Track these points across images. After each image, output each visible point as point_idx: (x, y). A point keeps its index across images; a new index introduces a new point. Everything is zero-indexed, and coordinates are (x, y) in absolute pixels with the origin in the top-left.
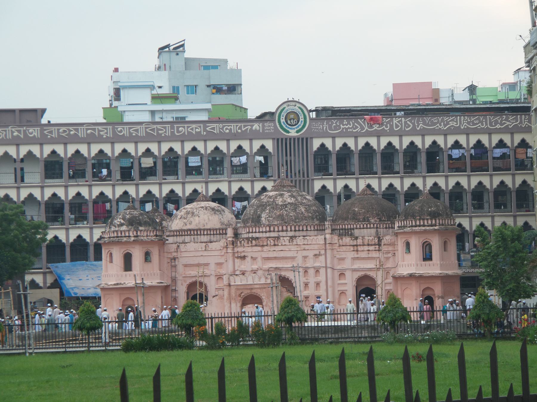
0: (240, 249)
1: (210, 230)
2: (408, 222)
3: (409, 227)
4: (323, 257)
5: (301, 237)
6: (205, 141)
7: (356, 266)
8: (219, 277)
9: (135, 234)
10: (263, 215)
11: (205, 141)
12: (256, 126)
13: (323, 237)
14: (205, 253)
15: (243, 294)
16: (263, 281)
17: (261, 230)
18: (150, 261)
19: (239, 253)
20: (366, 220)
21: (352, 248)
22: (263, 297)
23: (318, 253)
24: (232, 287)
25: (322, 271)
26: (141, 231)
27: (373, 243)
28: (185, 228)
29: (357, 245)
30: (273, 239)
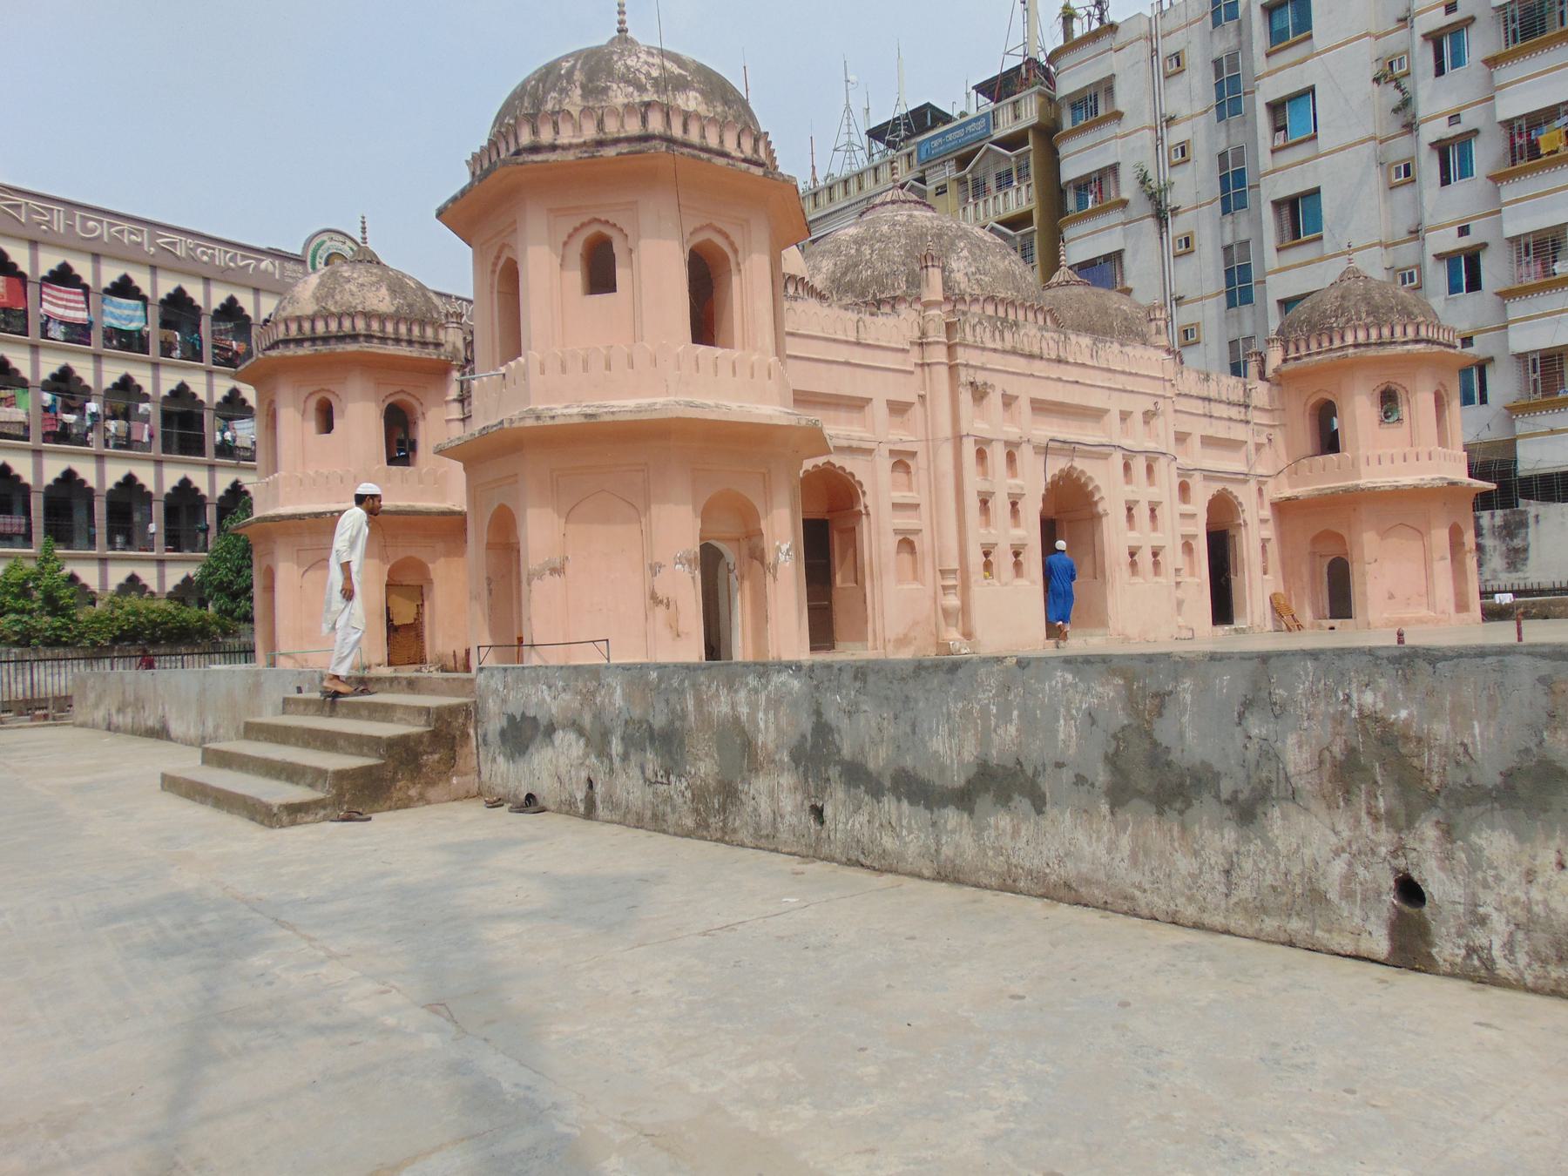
0: (974, 357)
2: (1398, 330)
3: (1405, 343)
5: (1116, 346)
7: (1209, 464)
8: (902, 462)
9: (747, 144)
10: (954, 265)
12: (266, 264)
14: (857, 355)
19: (971, 371)
21: (1199, 407)
23: (1152, 408)
25: (1161, 466)
27: (1234, 398)
29: (1210, 400)
30: (1056, 336)
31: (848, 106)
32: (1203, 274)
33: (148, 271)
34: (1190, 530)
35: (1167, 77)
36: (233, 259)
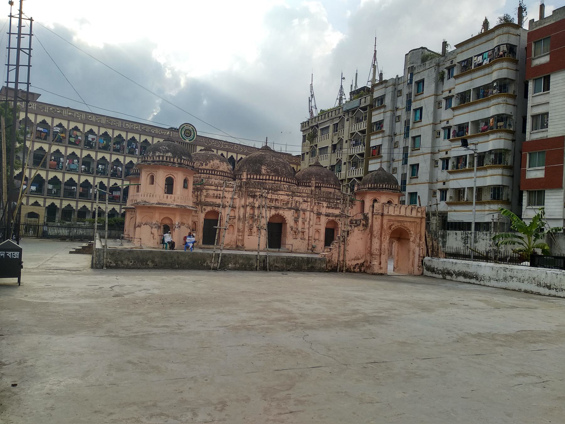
1: (222, 171)
4: (309, 203)
6: (140, 134)
9: (179, 160)
11: (140, 134)
13: (310, 188)
15: (393, 227)
16: (414, 213)
17: (261, 178)
18: (187, 188)
20: (328, 182)
22: (412, 232)
24: (385, 217)
25: (308, 214)
26: (184, 160)
28: (201, 167)
31: (342, 86)
32: (398, 154)
33: (139, 135)
34: (318, 227)
35: (398, 97)
36: (160, 132)
